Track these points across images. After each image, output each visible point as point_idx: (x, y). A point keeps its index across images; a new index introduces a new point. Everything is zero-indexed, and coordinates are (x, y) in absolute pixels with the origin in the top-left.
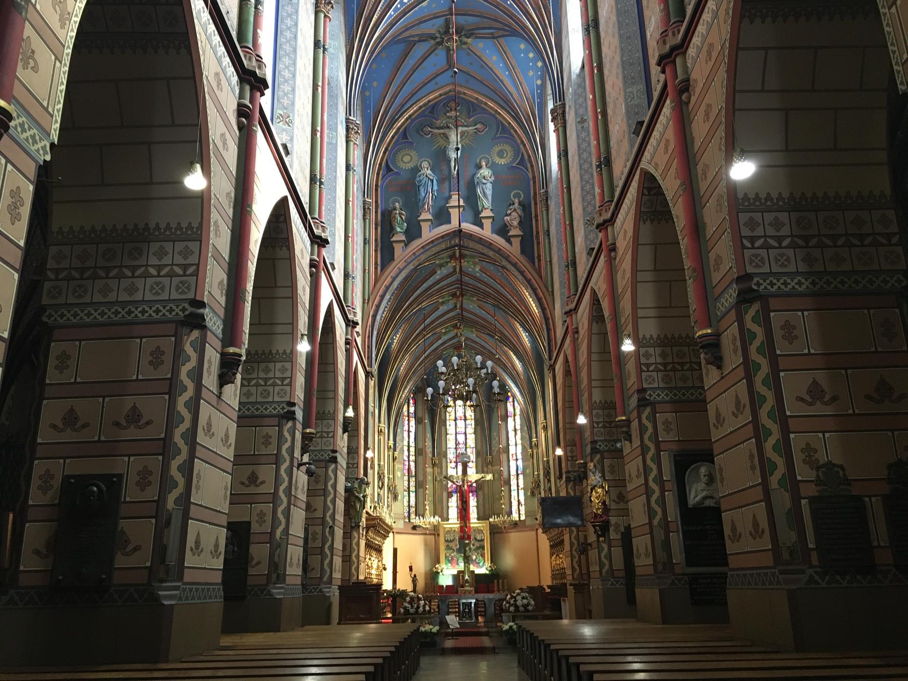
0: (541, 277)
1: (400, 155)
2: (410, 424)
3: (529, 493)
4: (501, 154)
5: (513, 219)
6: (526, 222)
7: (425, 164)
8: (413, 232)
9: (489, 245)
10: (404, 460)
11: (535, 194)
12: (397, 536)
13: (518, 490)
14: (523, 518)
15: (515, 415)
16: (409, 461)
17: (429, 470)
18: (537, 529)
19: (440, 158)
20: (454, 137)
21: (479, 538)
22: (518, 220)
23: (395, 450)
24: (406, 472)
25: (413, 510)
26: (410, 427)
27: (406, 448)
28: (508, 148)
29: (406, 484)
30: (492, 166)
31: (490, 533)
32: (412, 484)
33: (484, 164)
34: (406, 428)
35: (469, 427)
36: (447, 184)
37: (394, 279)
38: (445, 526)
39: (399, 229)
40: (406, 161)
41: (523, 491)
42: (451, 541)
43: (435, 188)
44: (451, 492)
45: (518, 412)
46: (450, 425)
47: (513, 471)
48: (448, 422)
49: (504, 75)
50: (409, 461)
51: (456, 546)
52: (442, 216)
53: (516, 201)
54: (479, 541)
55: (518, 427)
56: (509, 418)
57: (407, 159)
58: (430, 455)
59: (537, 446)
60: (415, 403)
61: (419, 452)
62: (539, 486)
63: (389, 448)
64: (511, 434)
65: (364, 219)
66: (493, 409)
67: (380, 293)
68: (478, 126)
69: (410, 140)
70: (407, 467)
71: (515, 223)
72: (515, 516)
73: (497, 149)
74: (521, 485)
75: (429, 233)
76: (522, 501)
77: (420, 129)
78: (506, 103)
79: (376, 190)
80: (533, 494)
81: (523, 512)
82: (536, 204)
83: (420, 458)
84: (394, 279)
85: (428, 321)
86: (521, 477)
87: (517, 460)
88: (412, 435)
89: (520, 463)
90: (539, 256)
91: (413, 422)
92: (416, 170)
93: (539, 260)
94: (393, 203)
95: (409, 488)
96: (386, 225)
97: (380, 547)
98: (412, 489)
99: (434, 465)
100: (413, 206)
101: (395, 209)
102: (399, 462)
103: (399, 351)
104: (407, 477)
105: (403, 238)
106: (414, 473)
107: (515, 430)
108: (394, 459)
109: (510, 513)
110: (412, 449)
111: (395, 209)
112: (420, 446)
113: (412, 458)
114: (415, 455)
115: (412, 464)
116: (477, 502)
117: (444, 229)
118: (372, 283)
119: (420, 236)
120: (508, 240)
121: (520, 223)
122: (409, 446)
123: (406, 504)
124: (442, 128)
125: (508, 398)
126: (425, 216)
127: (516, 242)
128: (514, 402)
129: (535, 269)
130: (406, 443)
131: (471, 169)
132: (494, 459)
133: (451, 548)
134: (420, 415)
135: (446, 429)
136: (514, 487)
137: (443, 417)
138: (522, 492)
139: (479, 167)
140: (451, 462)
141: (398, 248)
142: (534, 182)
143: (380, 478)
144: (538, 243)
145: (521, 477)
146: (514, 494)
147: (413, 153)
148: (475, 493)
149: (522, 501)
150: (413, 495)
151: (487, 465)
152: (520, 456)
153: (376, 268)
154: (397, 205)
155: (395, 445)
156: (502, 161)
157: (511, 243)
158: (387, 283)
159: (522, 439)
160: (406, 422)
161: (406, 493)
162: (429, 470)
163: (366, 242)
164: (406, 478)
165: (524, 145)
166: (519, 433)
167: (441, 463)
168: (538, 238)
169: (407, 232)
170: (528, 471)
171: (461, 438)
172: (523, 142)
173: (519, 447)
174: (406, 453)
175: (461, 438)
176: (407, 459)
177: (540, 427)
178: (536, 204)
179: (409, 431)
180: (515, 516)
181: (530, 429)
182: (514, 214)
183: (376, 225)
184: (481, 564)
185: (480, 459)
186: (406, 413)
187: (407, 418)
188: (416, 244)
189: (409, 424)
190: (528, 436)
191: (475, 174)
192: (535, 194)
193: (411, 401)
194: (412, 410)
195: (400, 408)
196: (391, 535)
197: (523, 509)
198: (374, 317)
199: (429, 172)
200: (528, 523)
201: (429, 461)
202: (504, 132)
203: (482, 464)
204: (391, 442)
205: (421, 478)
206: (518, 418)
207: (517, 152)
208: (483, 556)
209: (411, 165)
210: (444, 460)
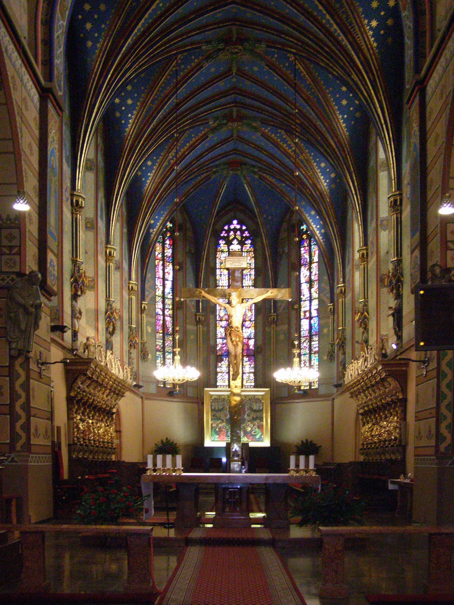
2: (166, 271)
3: (325, 358)
10: (157, 314)
13: (310, 354)
15: (311, 262)
16: (164, 315)
18: (333, 399)
21: (255, 407)
26: (166, 274)
27: (159, 299)
29: (159, 343)
31: (271, 403)
35: (247, 278)
38: (212, 393)
41: (317, 355)
42: (220, 410)
44: (221, 355)
45: (316, 259)
46: (221, 275)
48: (218, 272)
50: (164, 315)
51: (226, 415)
54: (255, 411)
56: (303, 269)
58: (193, 310)
64: (305, 287)
66: (281, 255)
70: (161, 322)
83: (180, 313)
86: (316, 338)
87: (311, 318)
88: (169, 284)
89: (315, 322)
91: (169, 268)
95: (164, 347)
102: (151, 316)
104: (161, 335)
110: (169, 302)
113: (168, 312)
114: (173, 309)
115: (169, 320)
116: (255, 367)
122: (164, 297)
128: (310, 246)
130: (159, 292)
132: (279, 318)
133: (219, 419)
134: (180, 257)
135: (216, 280)
137: (212, 265)
140: (221, 320)
148: (253, 358)
151: (270, 324)
152: (314, 313)
160: (161, 268)
170: (325, 331)
173: (315, 303)
174: (159, 305)
176: (161, 313)
179: (164, 279)
184: (257, 437)
185: (260, 317)
186: (160, 256)
187: (161, 263)
189: (163, 270)
190: (328, 288)
193: (168, 242)
194: (169, 252)
200: (321, 392)
203: (264, 323)
206: (315, 266)
208: (260, 427)
210: (212, 316)
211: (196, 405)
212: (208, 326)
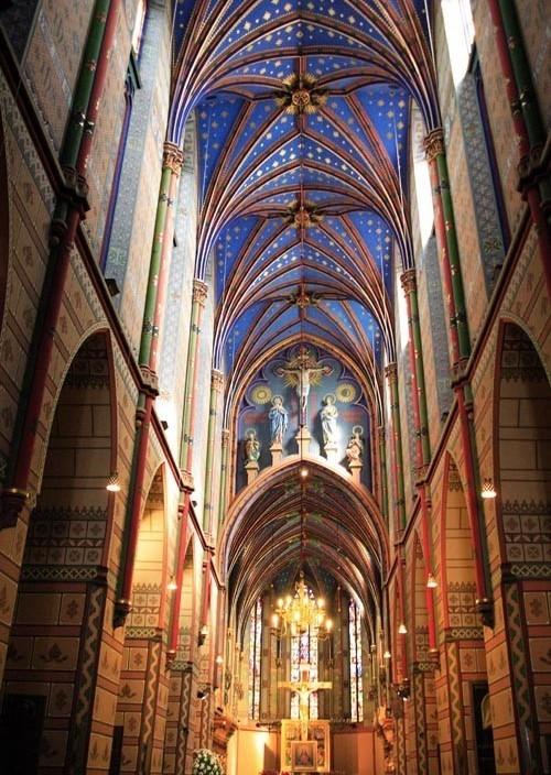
0: (378, 506)
1: (255, 393)
4: (344, 393)
5: (355, 452)
6: (367, 455)
7: (278, 401)
8: (266, 460)
9: (332, 474)
11: (374, 430)
12: (242, 733)
14: (361, 719)
17: (273, 670)
19: (292, 395)
20: (305, 377)
22: (358, 453)
23: (242, 650)
24: (251, 671)
25: (257, 708)
27: (252, 649)
28: (350, 388)
29: (251, 684)
30: (338, 404)
32: (257, 683)
33: (329, 401)
34: (253, 629)
36: (296, 419)
37: (247, 502)
39: (252, 458)
40: (261, 396)
43: (286, 421)
47: (353, 674)
49: (347, 329)
52: (292, 447)
53: (357, 435)
55: (359, 632)
57: (261, 395)
58: (275, 656)
59: (375, 651)
60: (262, 606)
61: (264, 653)
62: (376, 690)
63: (236, 649)
64: (352, 638)
65: (223, 448)
67: (235, 514)
68: (326, 368)
69: (265, 379)
71: (356, 455)
72: (354, 719)
73: (341, 388)
74: (360, 689)
75: (281, 461)
76: (361, 704)
77: (273, 370)
78: (350, 351)
79: (234, 422)
80: (371, 697)
81: (361, 714)
82: (374, 439)
83: (265, 660)
84: (247, 502)
85: (275, 534)
90: (376, 485)
91: (259, 624)
92: (269, 406)
93: (376, 490)
94: (249, 434)
96: (242, 453)
97: (225, 744)
98: (257, 688)
99: (278, 665)
100: (266, 436)
101: (250, 439)
103: (249, 560)
105: (256, 465)
106: (259, 673)
107: (356, 635)
108: (241, 659)
109: (349, 716)
110: (258, 650)
111: (250, 439)
112: (266, 647)
113: (258, 658)
115: (258, 664)
117: (294, 458)
118: (227, 505)
119: (270, 463)
120: (349, 471)
121: (360, 455)
123: (251, 702)
124: (294, 369)
125: (350, 604)
126: (277, 446)
127: (356, 472)
129: (373, 497)
130: (252, 643)
131: (319, 407)
136: (353, 690)
138: (360, 695)
139: (324, 404)
141: (251, 475)
142: (373, 419)
143: (227, 679)
144: (376, 474)
145: (360, 679)
146: (353, 696)
147: (268, 390)
149: (361, 704)
150: (257, 694)
152: (360, 660)
153: (231, 492)
154: (252, 436)
155: (242, 647)
156: (345, 400)
157: (351, 473)
158: (241, 506)
159: (362, 642)
161: (251, 692)
162: (273, 670)
163: (223, 468)
164: (252, 676)
165: (365, 386)
166: (359, 637)
167: (285, 664)
168: (375, 469)
169: (260, 461)
171: (305, 640)
172: (363, 384)
174: (252, 653)
175: (305, 640)
177: (378, 635)
178: (374, 439)
180: (354, 719)
181: (369, 634)
182: (355, 447)
183: (233, 452)
185: (322, 663)
188: (268, 471)
191: (321, 411)
192: (374, 430)
194: (259, 612)
195: (249, 611)
196: (236, 732)
197: (361, 711)
198: (228, 535)
199: (281, 407)
201: (273, 664)
202: (346, 374)
204: (239, 644)
205: (265, 678)
207: (359, 392)
209: (264, 401)
210: (288, 661)
211: (274, 735)
212: (285, 668)
